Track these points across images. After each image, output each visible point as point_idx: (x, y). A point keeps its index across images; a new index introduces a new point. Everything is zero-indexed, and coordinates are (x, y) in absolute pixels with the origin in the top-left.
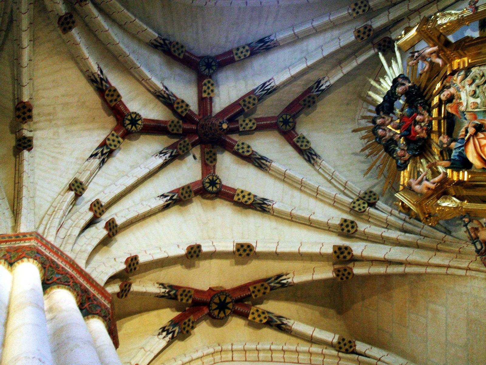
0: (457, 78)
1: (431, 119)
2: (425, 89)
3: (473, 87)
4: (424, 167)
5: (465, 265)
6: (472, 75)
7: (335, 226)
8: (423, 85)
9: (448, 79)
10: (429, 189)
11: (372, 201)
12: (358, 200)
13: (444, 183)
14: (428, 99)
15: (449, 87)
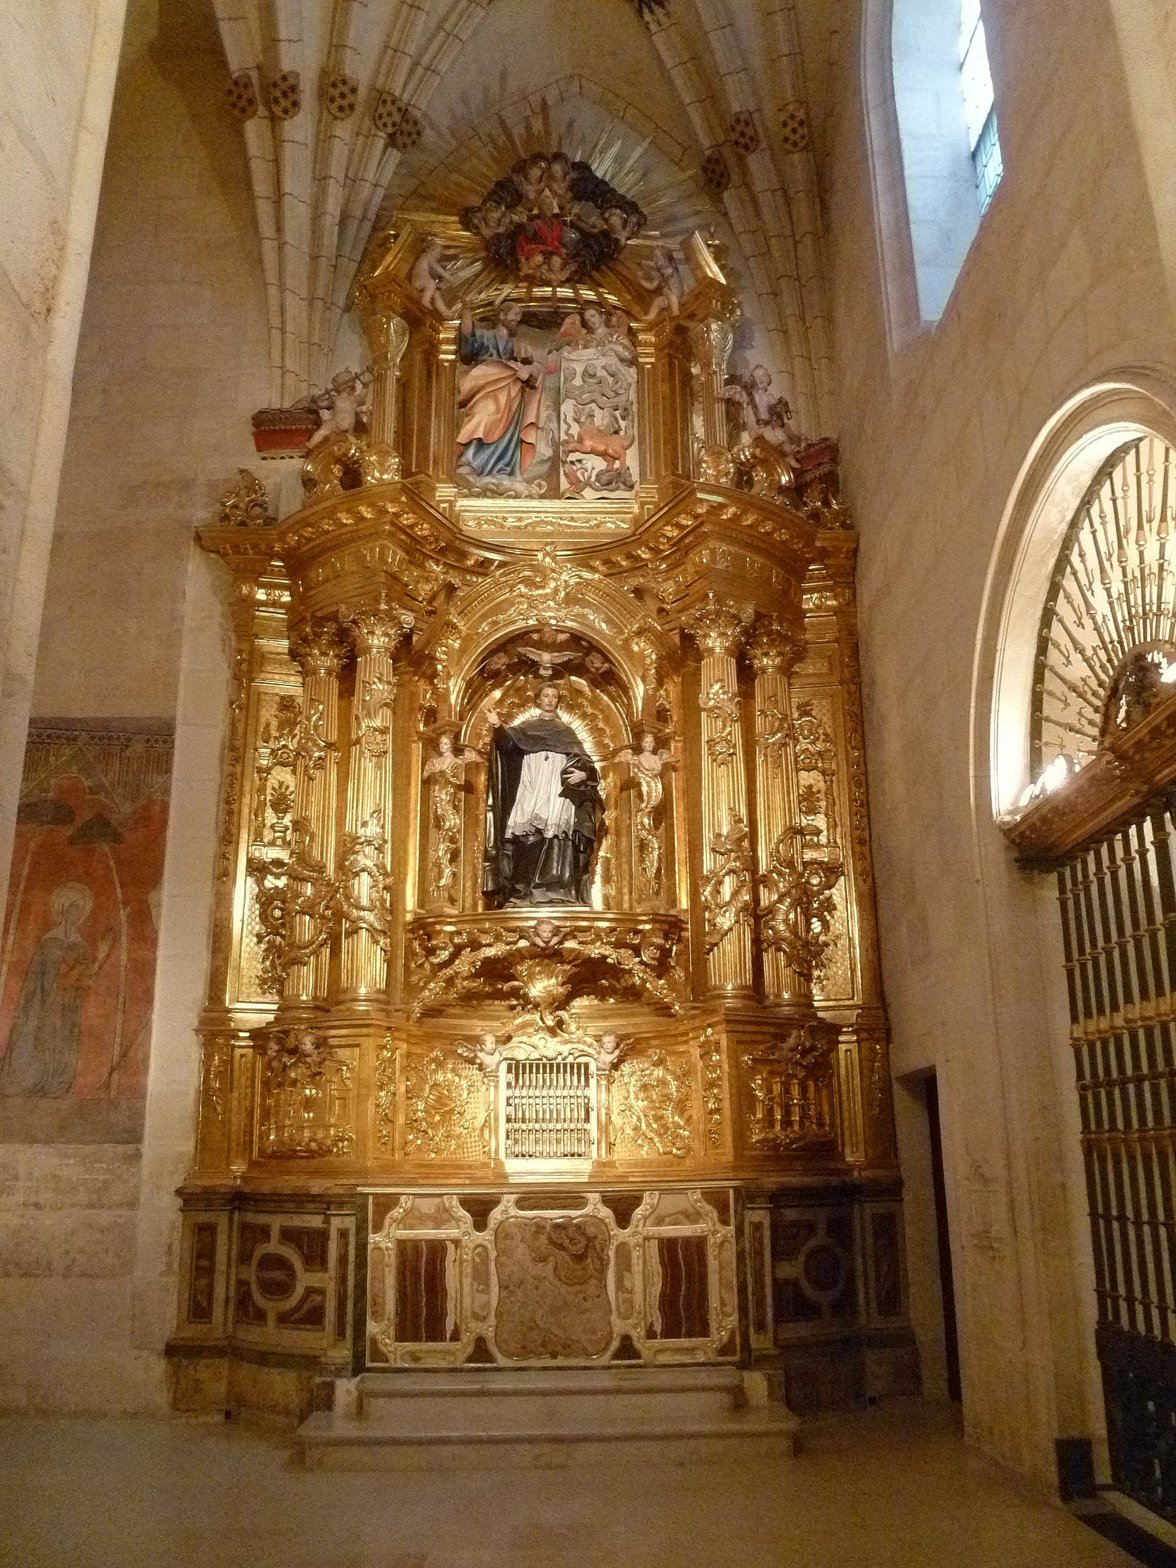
0: (619, 345)
1: (554, 284)
2: (612, 270)
3: (601, 373)
4: (465, 270)
5: (289, 364)
6: (623, 369)
7: (339, 63)
8: (619, 267)
9: (625, 318)
10: (422, 291)
11: (400, 140)
12: (399, 110)
13: (433, 317)
14: (590, 277)
15: (608, 324)
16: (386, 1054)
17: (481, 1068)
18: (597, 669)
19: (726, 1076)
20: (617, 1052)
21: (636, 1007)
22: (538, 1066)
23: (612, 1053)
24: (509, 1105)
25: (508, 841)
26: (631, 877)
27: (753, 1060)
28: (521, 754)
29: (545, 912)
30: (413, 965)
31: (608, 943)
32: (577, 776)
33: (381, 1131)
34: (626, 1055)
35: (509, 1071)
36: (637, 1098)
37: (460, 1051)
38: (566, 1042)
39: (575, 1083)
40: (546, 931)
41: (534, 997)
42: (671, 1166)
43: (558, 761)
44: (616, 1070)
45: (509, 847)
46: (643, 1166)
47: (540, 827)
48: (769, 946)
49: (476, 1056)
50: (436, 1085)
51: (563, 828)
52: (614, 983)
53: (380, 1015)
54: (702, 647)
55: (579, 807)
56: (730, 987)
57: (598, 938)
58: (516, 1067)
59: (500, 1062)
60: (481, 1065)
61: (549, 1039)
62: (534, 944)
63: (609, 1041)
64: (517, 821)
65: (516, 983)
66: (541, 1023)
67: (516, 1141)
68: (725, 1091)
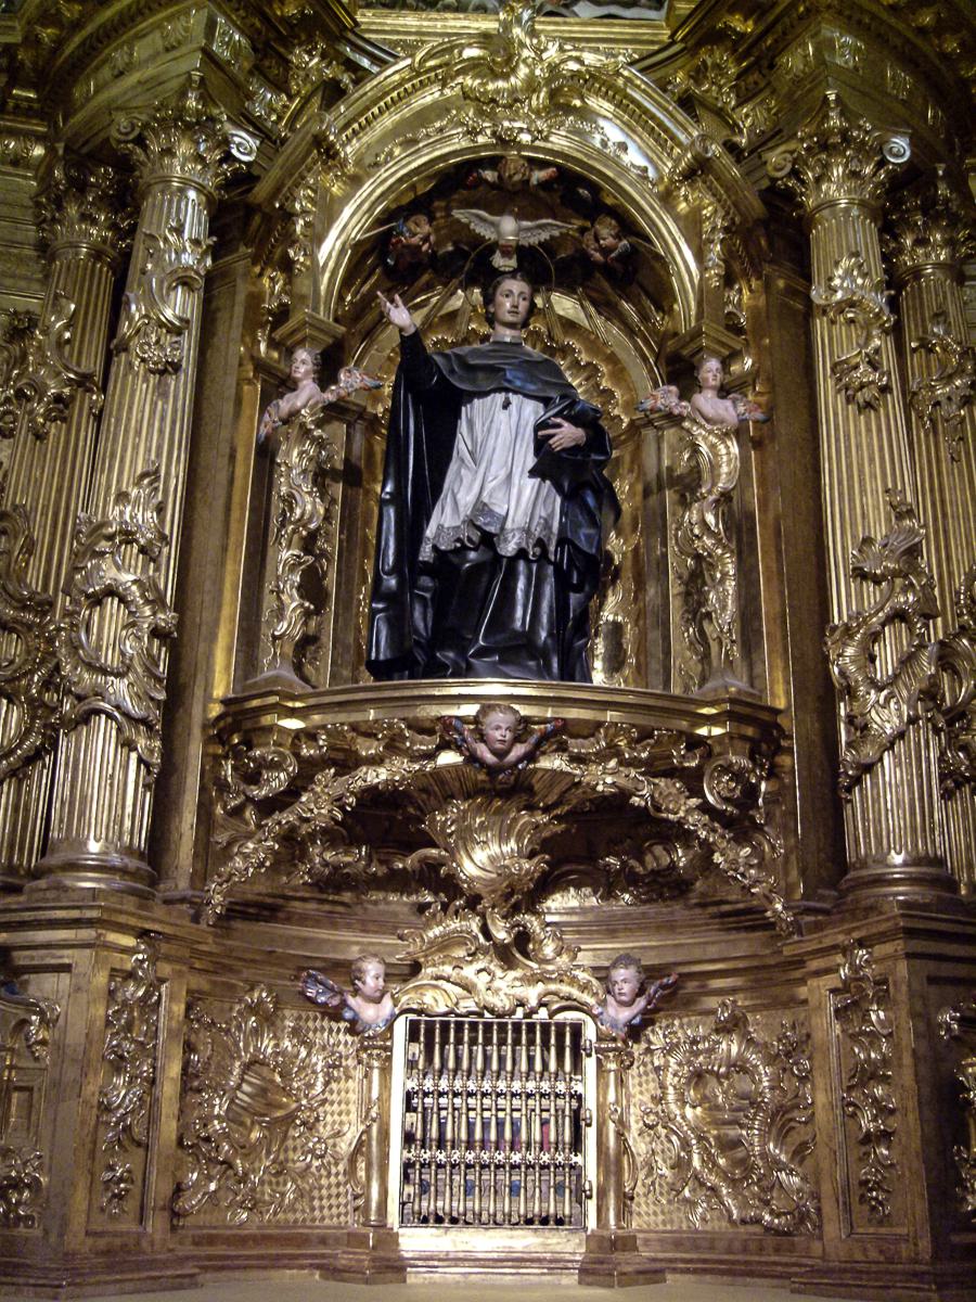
16: (132, 991)
17: (354, 1028)
18: (605, 251)
19: (907, 1060)
20: (641, 1003)
21: (678, 910)
22: (474, 1026)
23: (629, 1004)
24: (409, 1108)
25: (427, 568)
26: (667, 652)
27: (960, 1021)
28: (460, 398)
29: (494, 687)
30: (219, 810)
31: (634, 763)
32: (567, 434)
33: (111, 1168)
34: (656, 1010)
35: (413, 1035)
36: (682, 1101)
37: (311, 993)
38: (532, 980)
39: (553, 1066)
40: (499, 726)
41: (471, 880)
42: (761, 1250)
43: (530, 411)
44: (637, 1040)
45: (425, 581)
46: (697, 1248)
47: (492, 529)
48: (959, 786)
49: (344, 1004)
50: (253, 1064)
51: (537, 532)
52: (632, 862)
53: (130, 904)
54: (811, 202)
55: (571, 497)
56: (898, 859)
57: (613, 751)
58: (429, 1032)
59: (394, 1017)
60: (354, 1022)
61: (499, 973)
62: (472, 758)
63: (625, 978)
64: (444, 522)
65: (434, 851)
66: (482, 939)
67: (424, 1188)
68: (900, 1091)
